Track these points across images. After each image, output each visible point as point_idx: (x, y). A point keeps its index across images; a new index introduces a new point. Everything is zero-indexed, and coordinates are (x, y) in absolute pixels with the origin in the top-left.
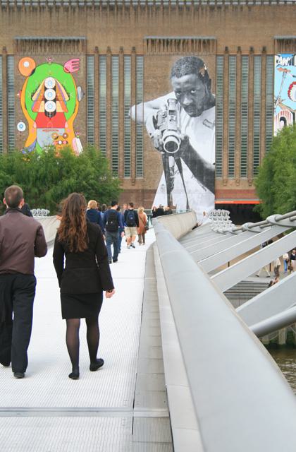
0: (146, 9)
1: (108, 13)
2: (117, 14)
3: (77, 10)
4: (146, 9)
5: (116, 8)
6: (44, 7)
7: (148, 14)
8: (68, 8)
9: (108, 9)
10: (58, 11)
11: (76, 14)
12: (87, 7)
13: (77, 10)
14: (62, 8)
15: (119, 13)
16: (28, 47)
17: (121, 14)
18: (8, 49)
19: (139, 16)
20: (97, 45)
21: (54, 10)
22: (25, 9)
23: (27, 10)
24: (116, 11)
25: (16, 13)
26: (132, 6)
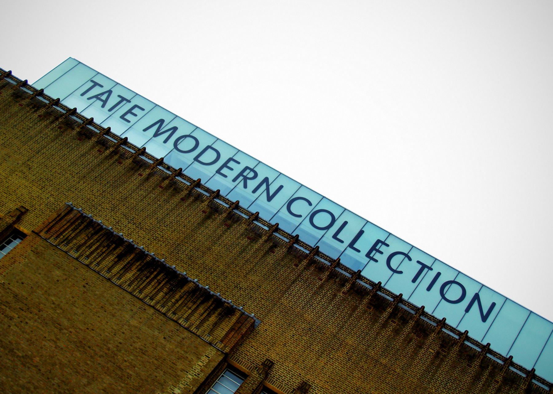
0: (477, 363)
1: (361, 307)
2: (384, 326)
3: (280, 252)
4: (477, 363)
5: (389, 310)
6: (199, 197)
7: (477, 378)
8: (260, 236)
9: (365, 301)
10: (229, 227)
11: (270, 259)
12: (312, 262)
13: (280, 252)
14: (244, 226)
15: (392, 326)
16: (81, 239)
17: (397, 332)
18: (29, 218)
19: (445, 367)
20: (273, 356)
21: (220, 218)
22: (150, 175)
23: (154, 180)
24: (385, 315)
25: (120, 169)
26: (440, 331)
